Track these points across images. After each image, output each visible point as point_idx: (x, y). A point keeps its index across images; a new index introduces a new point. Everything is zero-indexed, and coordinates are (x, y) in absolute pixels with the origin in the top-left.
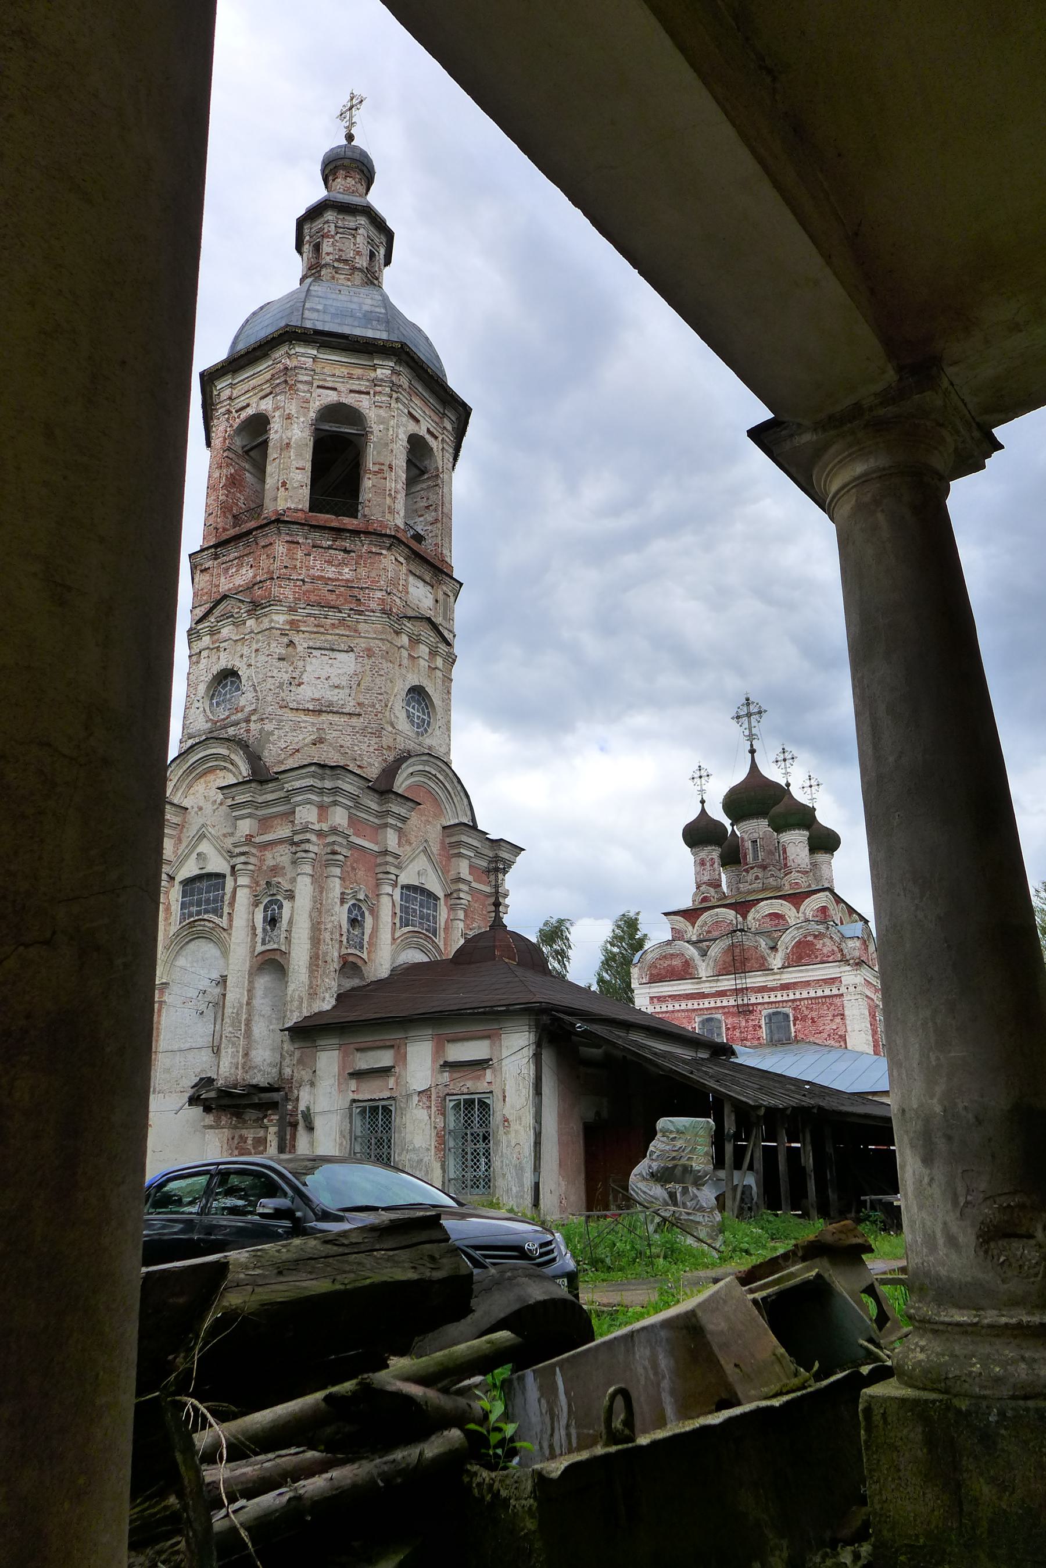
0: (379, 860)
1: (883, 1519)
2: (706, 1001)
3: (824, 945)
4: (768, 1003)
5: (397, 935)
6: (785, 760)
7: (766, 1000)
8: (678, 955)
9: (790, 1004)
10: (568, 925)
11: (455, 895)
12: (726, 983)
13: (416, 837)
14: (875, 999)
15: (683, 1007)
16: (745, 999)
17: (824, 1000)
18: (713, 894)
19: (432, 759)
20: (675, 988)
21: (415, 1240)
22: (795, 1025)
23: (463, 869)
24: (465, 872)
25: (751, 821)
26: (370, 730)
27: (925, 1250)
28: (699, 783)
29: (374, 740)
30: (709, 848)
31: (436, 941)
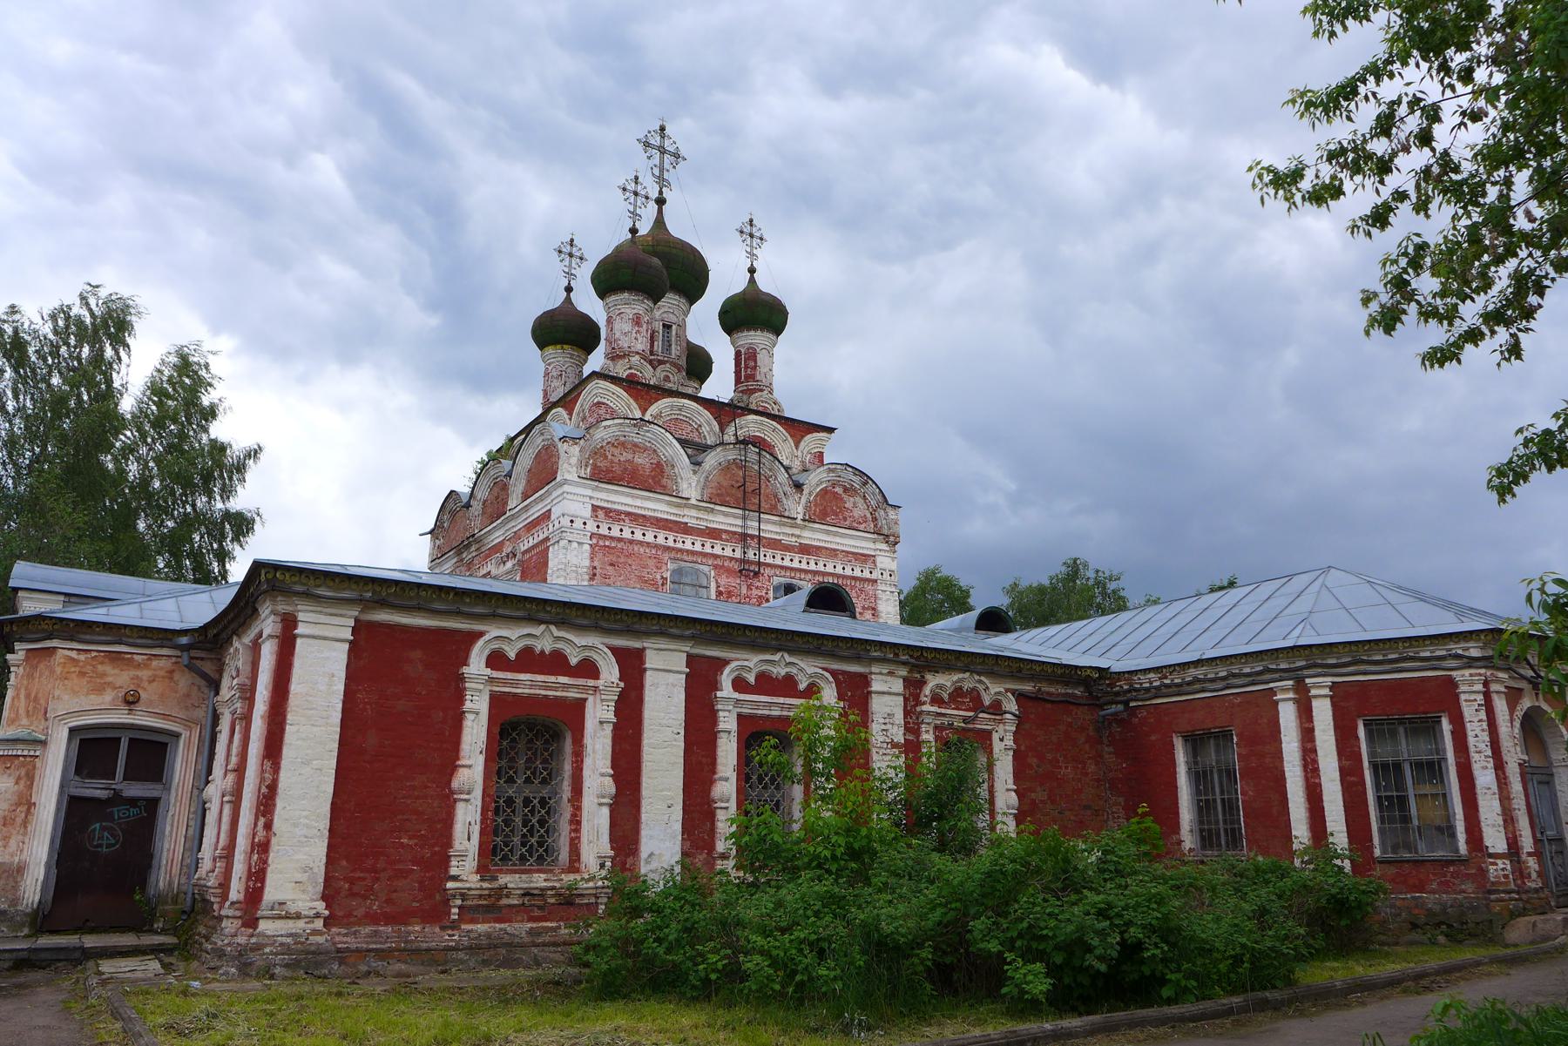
2: (689, 540)
3: (855, 505)
7: (778, 561)
12: (721, 518)
15: (649, 538)
20: (638, 503)
28: (632, 200)
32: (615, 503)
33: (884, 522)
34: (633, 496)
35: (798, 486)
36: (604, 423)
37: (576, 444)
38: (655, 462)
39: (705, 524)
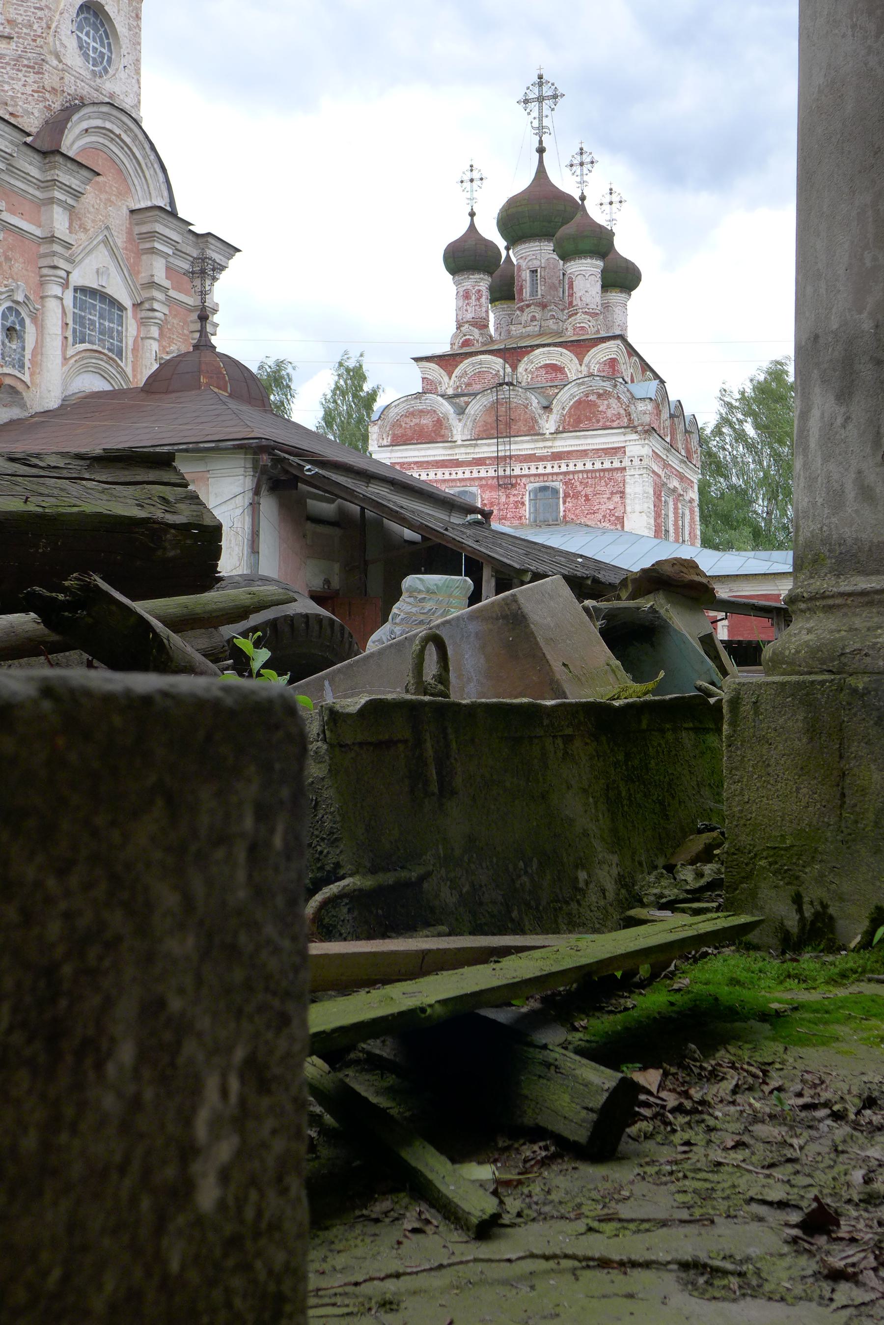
0: (43, 249)
1: (742, 822)
2: (460, 470)
3: (609, 407)
4: (535, 475)
5: (70, 352)
6: (582, 164)
7: (533, 471)
8: (428, 412)
9: (561, 477)
10: (290, 370)
11: (147, 306)
12: (486, 449)
13: (93, 221)
14: (663, 476)
16: (508, 469)
17: (602, 474)
18: (477, 337)
19: (115, 112)
20: (423, 453)
21: (139, 478)
22: (564, 503)
23: (158, 270)
24: (160, 276)
25: (532, 244)
26: (26, 62)
27: (826, 511)
28: (469, 189)
29: (32, 77)
30: (477, 276)
31: (122, 365)
34: (418, 450)
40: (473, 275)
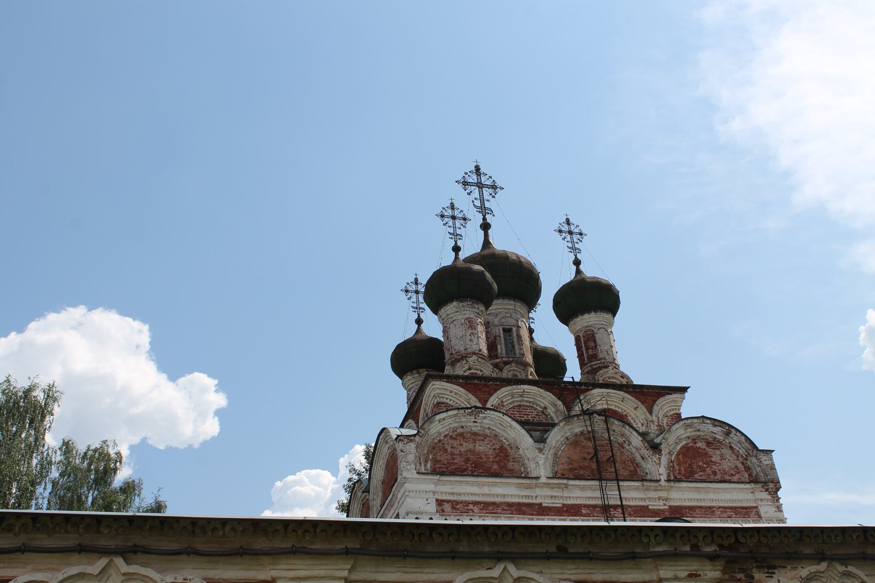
8: (486, 436)
12: (577, 493)
20: (486, 490)
25: (506, 301)
32: (460, 494)
33: (758, 469)
34: (479, 485)
35: (655, 448)
36: (438, 417)
37: (411, 441)
38: (498, 446)
39: (561, 501)
40: (477, 304)
